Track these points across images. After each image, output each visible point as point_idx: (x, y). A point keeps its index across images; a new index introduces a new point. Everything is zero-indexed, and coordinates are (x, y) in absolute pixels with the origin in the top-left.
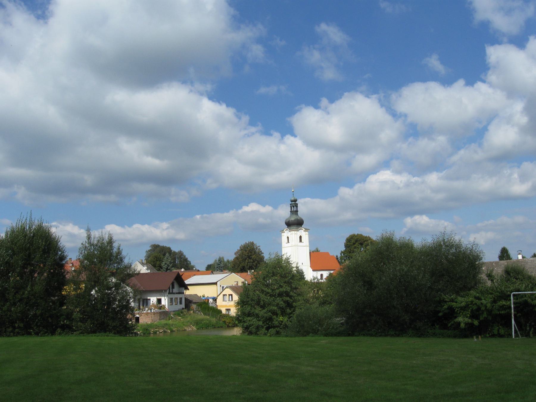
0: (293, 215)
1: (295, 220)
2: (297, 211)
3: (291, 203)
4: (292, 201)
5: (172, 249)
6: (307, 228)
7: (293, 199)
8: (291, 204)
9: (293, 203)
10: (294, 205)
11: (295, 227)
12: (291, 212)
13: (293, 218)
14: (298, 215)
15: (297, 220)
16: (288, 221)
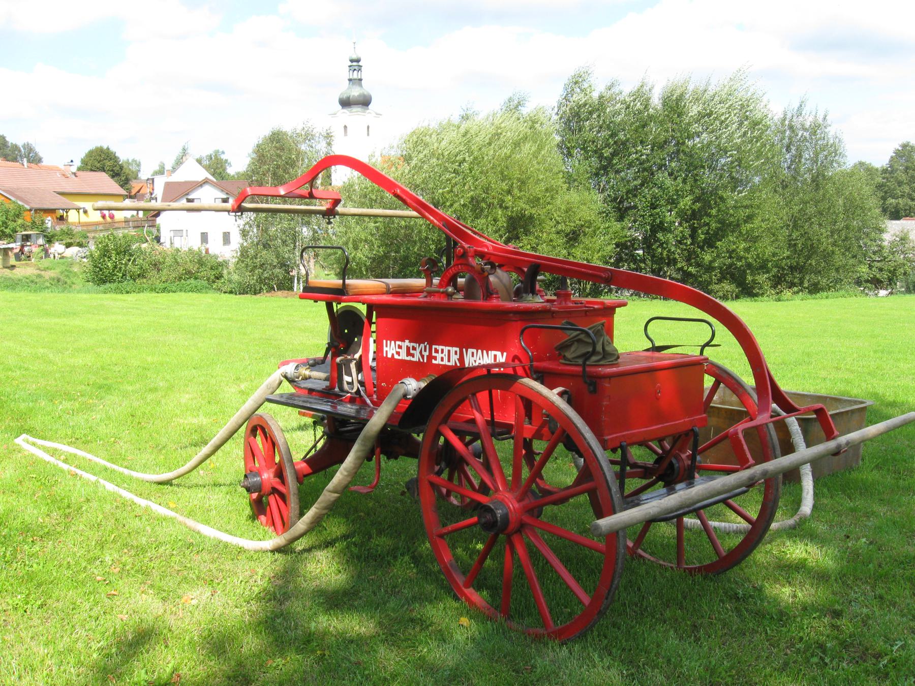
0: (354, 86)
1: (359, 96)
2: (361, 80)
3: (350, 64)
4: (352, 61)
5: (7, 139)
6: (378, 112)
7: (354, 57)
8: (350, 66)
9: (355, 64)
10: (356, 68)
11: (359, 109)
12: (350, 80)
13: (355, 92)
14: (361, 85)
15: (364, 96)
16: (345, 96)
